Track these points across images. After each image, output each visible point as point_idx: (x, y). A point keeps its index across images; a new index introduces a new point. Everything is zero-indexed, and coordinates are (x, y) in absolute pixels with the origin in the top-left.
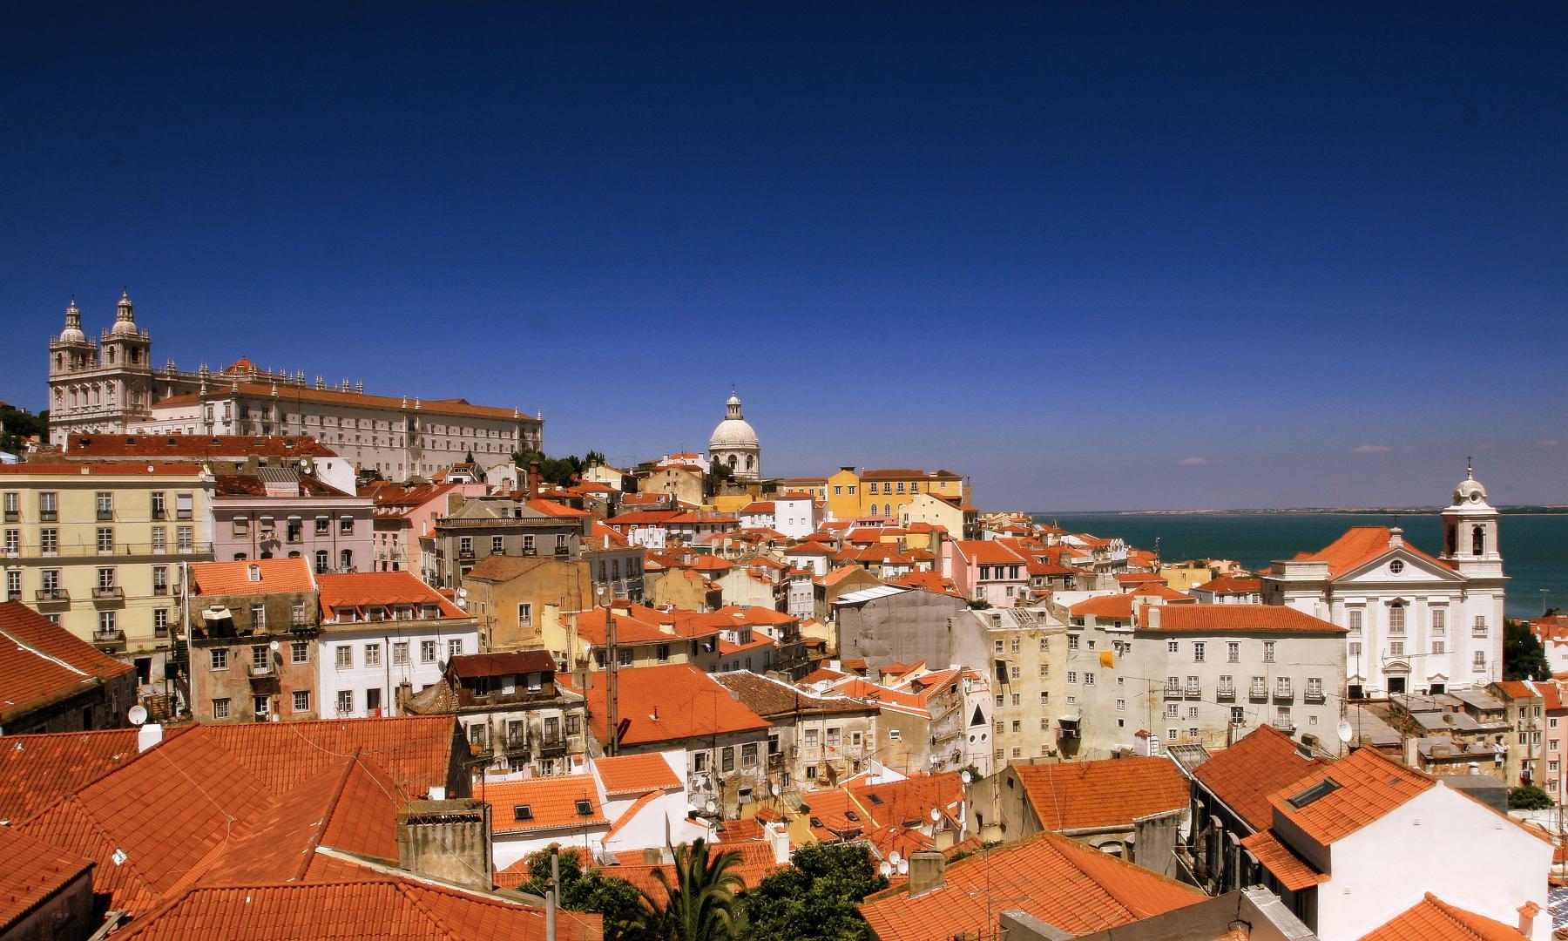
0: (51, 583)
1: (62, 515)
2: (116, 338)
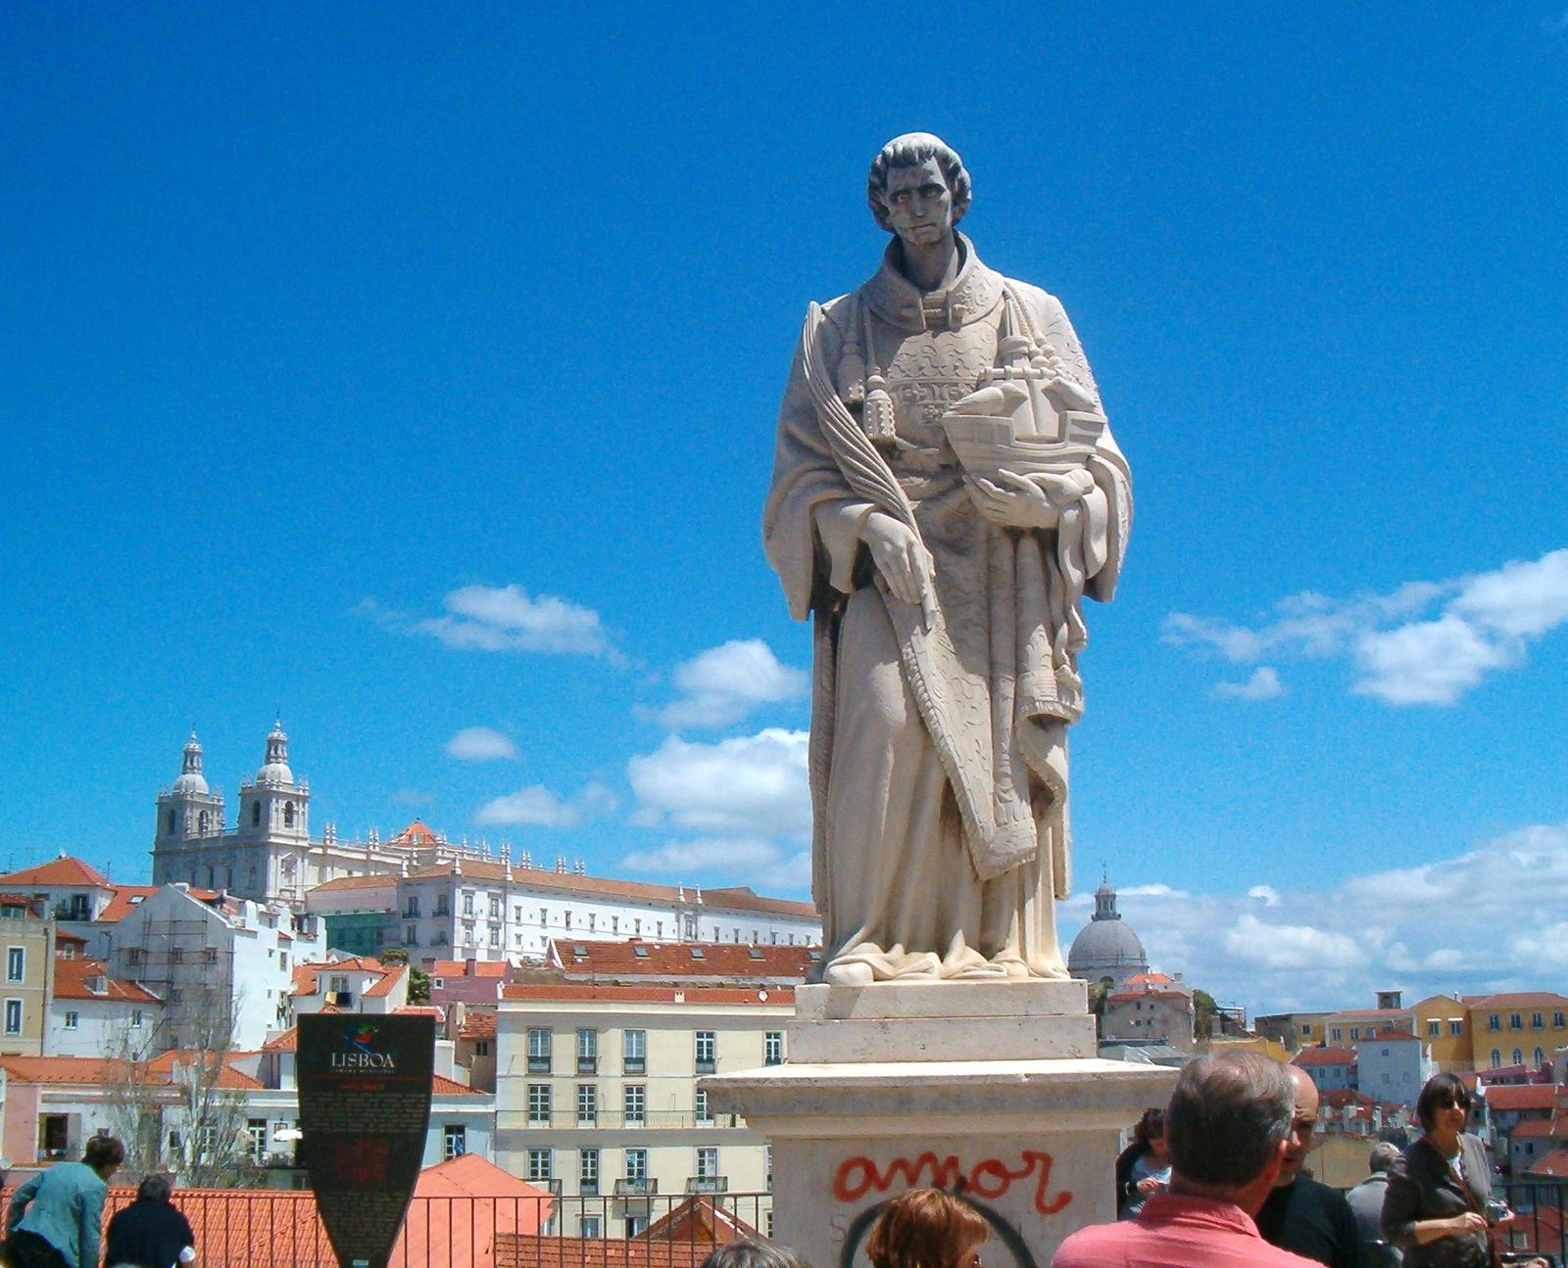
0: (636, 1168)
1: (651, 1066)
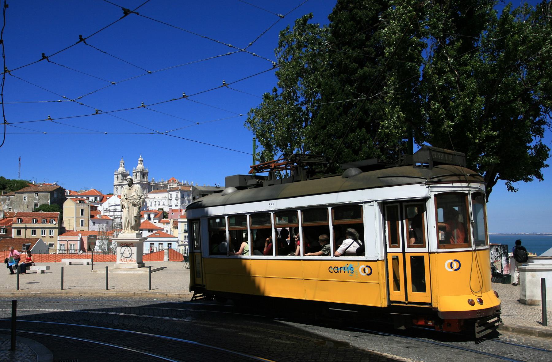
2: (138, 171)
